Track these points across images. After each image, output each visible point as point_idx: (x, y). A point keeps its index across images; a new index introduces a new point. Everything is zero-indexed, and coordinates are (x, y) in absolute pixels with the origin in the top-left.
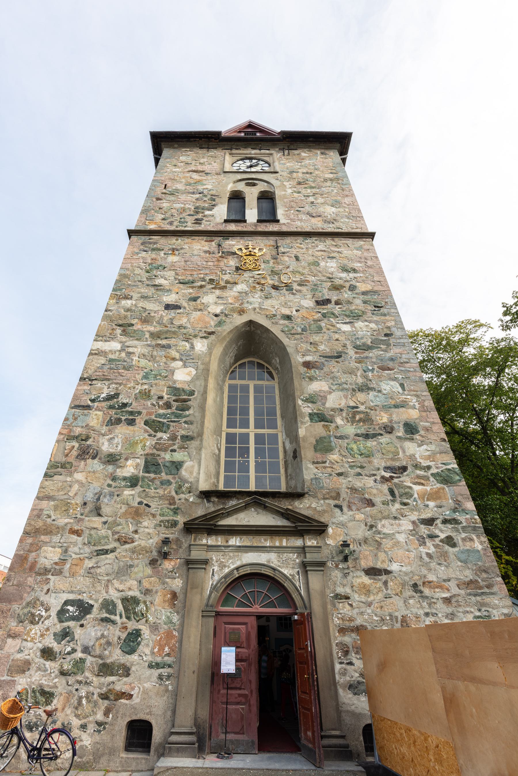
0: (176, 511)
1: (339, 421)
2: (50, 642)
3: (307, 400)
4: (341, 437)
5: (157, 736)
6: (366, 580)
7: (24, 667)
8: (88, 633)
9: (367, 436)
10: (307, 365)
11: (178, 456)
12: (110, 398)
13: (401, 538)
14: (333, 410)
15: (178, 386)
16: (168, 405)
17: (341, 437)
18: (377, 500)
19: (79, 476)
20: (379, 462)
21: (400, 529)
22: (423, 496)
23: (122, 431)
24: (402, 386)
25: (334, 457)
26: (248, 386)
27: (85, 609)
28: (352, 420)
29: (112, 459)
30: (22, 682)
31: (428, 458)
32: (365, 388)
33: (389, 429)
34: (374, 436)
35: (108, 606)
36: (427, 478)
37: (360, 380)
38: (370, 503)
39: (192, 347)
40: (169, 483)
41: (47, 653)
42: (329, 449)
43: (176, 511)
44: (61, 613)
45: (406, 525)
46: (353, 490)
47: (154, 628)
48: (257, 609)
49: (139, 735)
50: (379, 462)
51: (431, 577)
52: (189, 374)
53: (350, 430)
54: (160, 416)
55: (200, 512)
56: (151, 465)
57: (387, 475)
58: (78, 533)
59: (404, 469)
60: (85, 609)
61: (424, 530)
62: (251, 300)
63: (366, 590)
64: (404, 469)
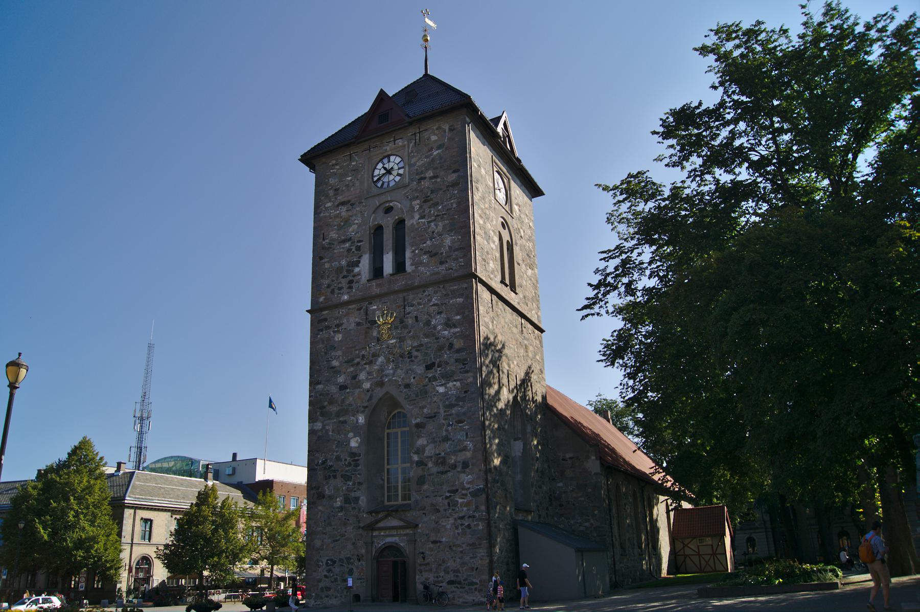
0: (359, 522)
1: (430, 465)
2: (325, 573)
3: (415, 453)
4: (430, 475)
5: (362, 598)
6: (431, 545)
7: (320, 581)
8: (337, 569)
9: (442, 473)
10: (418, 426)
11: (357, 494)
12: (324, 463)
13: (448, 527)
14: (428, 457)
15: (354, 450)
16: (350, 464)
17: (430, 475)
18: (441, 509)
19: (320, 508)
20: (445, 487)
21: (448, 524)
22: (462, 504)
23: (332, 482)
24: (467, 434)
25: (426, 487)
26: (397, 433)
27: (334, 562)
28: (436, 464)
29: (331, 497)
30: (321, 585)
31: (468, 483)
32: (446, 439)
33: (454, 467)
34: (446, 472)
35: (341, 560)
36: (466, 495)
37: (444, 434)
38: (438, 511)
39: (357, 422)
40: (354, 508)
41: (326, 576)
42: (423, 483)
43: (359, 522)
44: (327, 563)
45: (451, 521)
46: (432, 505)
47: (357, 568)
48: (392, 559)
49: (357, 598)
50: (445, 487)
51: (458, 542)
52: (357, 442)
53: (435, 470)
54: (346, 471)
55: (368, 521)
56: (347, 500)
57: (448, 495)
58: (325, 534)
59: (457, 490)
60: (334, 562)
61: (459, 522)
62: (387, 372)
63: (431, 550)
64: (457, 490)
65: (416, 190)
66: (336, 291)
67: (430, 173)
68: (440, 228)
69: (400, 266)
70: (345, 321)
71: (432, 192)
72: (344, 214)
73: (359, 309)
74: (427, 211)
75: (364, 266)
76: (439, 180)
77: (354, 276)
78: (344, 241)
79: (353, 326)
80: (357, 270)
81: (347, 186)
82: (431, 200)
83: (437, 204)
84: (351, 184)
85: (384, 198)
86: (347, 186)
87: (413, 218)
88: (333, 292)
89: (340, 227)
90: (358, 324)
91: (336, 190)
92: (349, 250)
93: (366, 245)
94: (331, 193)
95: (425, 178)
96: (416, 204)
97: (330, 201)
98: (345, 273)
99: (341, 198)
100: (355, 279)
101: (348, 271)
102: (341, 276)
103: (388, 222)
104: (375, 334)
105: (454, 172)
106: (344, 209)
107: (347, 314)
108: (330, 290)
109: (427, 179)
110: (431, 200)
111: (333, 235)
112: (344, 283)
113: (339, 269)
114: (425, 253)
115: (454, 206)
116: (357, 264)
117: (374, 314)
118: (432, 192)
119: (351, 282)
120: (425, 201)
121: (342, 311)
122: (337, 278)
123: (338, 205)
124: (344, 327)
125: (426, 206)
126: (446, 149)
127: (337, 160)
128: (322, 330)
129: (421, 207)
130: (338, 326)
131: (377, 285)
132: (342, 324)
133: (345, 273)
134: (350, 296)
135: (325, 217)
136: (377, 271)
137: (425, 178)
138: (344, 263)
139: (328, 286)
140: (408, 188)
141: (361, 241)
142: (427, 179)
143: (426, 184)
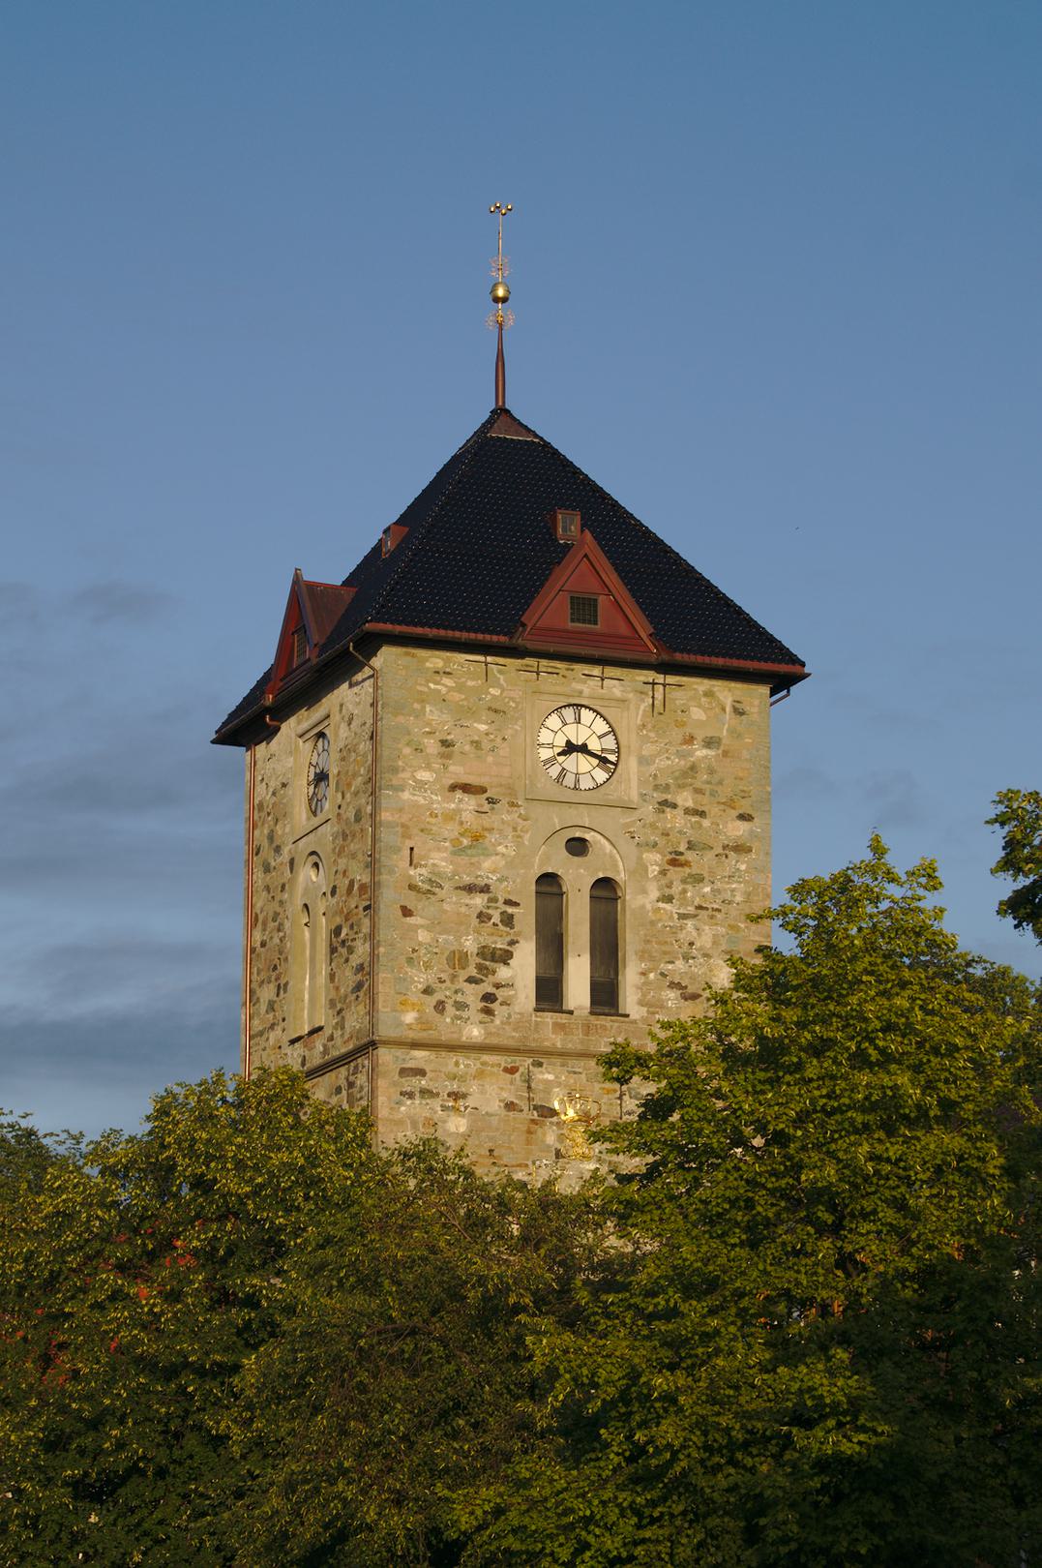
65: (652, 825)
66: (450, 1010)
67: (685, 799)
68: (705, 941)
69: (605, 996)
70: (474, 1089)
71: (691, 846)
72: (468, 816)
73: (512, 1071)
74: (677, 888)
75: (523, 969)
76: (706, 823)
77: (498, 986)
78: (470, 889)
79: (495, 1106)
80: (503, 973)
81: (476, 744)
82: (686, 864)
83: (699, 879)
84: (486, 745)
85: (573, 816)
86: (476, 744)
87: (644, 892)
88: (440, 1007)
89: (459, 851)
90: (510, 1106)
91: (445, 743)
92: (483, 917)
93: (526, 916)
94: (432, 746)
95: (675, 806)
96: (654, 860)
97: (428, 767)
98: (473, 971)
99: (458, 772)
100: (501, 994)
101: (480, 968)
102: (463, 975)
103: (578, 879)
104: (551, 1138)
105: (742, 817)
106: (470, 803)
107: (480, 1075)
108: (432, 1000)
109: (679, 811)
110: (686, 864)
111: (440, 860)
112: (472, 995)
113: (458, 959)
114: (673, 985)
115: (739, 898)
116: (505, 957)
117: (548, 1092)
118: (691, 846)
119: (489, 998)
120: (673, 863)
121: (465, 1063)
122: (454, 977)
123: (453, 788)
124: (471, 1102)
125: (675, 874)
126: (725, 754)
127: (447, 661)
128: (411, 1095)
129: (663, 873)
130: (456, 1096)
131: (556, 1025)
132: (464, 1096)
133: (473, 971)
134: (489, 1034)
135: (416, 805)
136: (549, 992)
137: (675, 806)
138: (470, 944)
139: (428, 991)
140: (636, 815)
141: (516, 904)
142: (679, 811)
143: (676, 820)
